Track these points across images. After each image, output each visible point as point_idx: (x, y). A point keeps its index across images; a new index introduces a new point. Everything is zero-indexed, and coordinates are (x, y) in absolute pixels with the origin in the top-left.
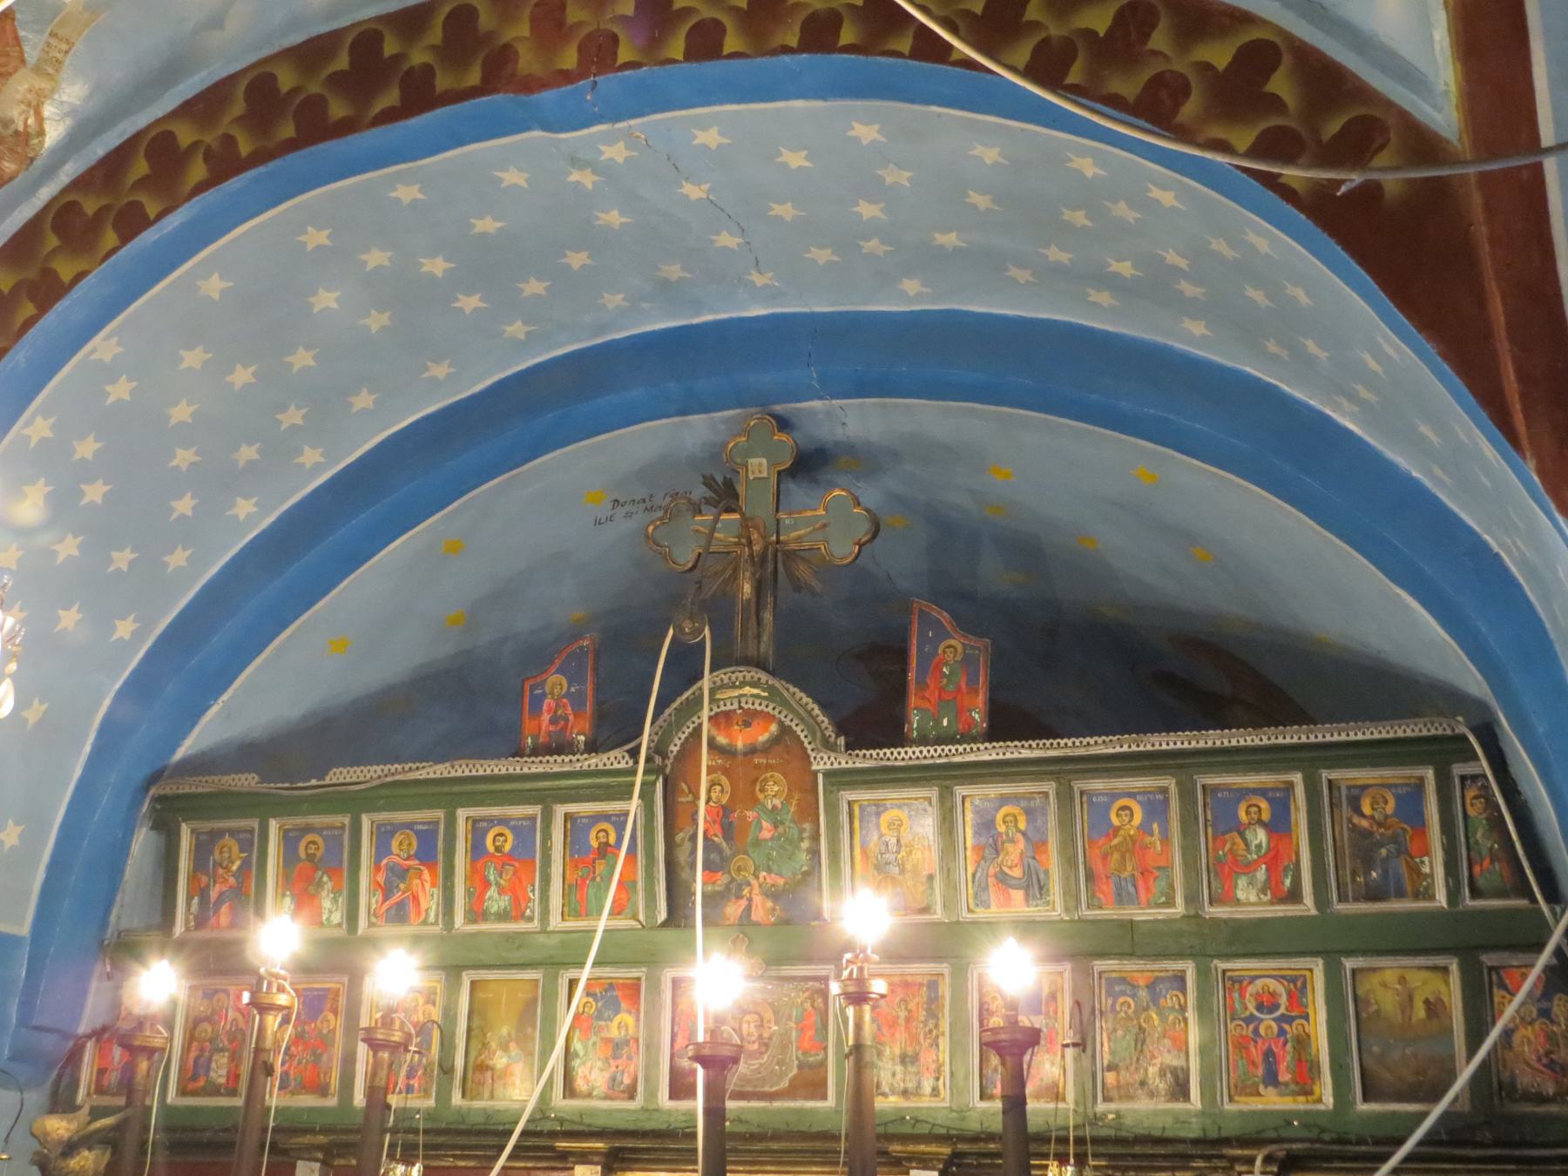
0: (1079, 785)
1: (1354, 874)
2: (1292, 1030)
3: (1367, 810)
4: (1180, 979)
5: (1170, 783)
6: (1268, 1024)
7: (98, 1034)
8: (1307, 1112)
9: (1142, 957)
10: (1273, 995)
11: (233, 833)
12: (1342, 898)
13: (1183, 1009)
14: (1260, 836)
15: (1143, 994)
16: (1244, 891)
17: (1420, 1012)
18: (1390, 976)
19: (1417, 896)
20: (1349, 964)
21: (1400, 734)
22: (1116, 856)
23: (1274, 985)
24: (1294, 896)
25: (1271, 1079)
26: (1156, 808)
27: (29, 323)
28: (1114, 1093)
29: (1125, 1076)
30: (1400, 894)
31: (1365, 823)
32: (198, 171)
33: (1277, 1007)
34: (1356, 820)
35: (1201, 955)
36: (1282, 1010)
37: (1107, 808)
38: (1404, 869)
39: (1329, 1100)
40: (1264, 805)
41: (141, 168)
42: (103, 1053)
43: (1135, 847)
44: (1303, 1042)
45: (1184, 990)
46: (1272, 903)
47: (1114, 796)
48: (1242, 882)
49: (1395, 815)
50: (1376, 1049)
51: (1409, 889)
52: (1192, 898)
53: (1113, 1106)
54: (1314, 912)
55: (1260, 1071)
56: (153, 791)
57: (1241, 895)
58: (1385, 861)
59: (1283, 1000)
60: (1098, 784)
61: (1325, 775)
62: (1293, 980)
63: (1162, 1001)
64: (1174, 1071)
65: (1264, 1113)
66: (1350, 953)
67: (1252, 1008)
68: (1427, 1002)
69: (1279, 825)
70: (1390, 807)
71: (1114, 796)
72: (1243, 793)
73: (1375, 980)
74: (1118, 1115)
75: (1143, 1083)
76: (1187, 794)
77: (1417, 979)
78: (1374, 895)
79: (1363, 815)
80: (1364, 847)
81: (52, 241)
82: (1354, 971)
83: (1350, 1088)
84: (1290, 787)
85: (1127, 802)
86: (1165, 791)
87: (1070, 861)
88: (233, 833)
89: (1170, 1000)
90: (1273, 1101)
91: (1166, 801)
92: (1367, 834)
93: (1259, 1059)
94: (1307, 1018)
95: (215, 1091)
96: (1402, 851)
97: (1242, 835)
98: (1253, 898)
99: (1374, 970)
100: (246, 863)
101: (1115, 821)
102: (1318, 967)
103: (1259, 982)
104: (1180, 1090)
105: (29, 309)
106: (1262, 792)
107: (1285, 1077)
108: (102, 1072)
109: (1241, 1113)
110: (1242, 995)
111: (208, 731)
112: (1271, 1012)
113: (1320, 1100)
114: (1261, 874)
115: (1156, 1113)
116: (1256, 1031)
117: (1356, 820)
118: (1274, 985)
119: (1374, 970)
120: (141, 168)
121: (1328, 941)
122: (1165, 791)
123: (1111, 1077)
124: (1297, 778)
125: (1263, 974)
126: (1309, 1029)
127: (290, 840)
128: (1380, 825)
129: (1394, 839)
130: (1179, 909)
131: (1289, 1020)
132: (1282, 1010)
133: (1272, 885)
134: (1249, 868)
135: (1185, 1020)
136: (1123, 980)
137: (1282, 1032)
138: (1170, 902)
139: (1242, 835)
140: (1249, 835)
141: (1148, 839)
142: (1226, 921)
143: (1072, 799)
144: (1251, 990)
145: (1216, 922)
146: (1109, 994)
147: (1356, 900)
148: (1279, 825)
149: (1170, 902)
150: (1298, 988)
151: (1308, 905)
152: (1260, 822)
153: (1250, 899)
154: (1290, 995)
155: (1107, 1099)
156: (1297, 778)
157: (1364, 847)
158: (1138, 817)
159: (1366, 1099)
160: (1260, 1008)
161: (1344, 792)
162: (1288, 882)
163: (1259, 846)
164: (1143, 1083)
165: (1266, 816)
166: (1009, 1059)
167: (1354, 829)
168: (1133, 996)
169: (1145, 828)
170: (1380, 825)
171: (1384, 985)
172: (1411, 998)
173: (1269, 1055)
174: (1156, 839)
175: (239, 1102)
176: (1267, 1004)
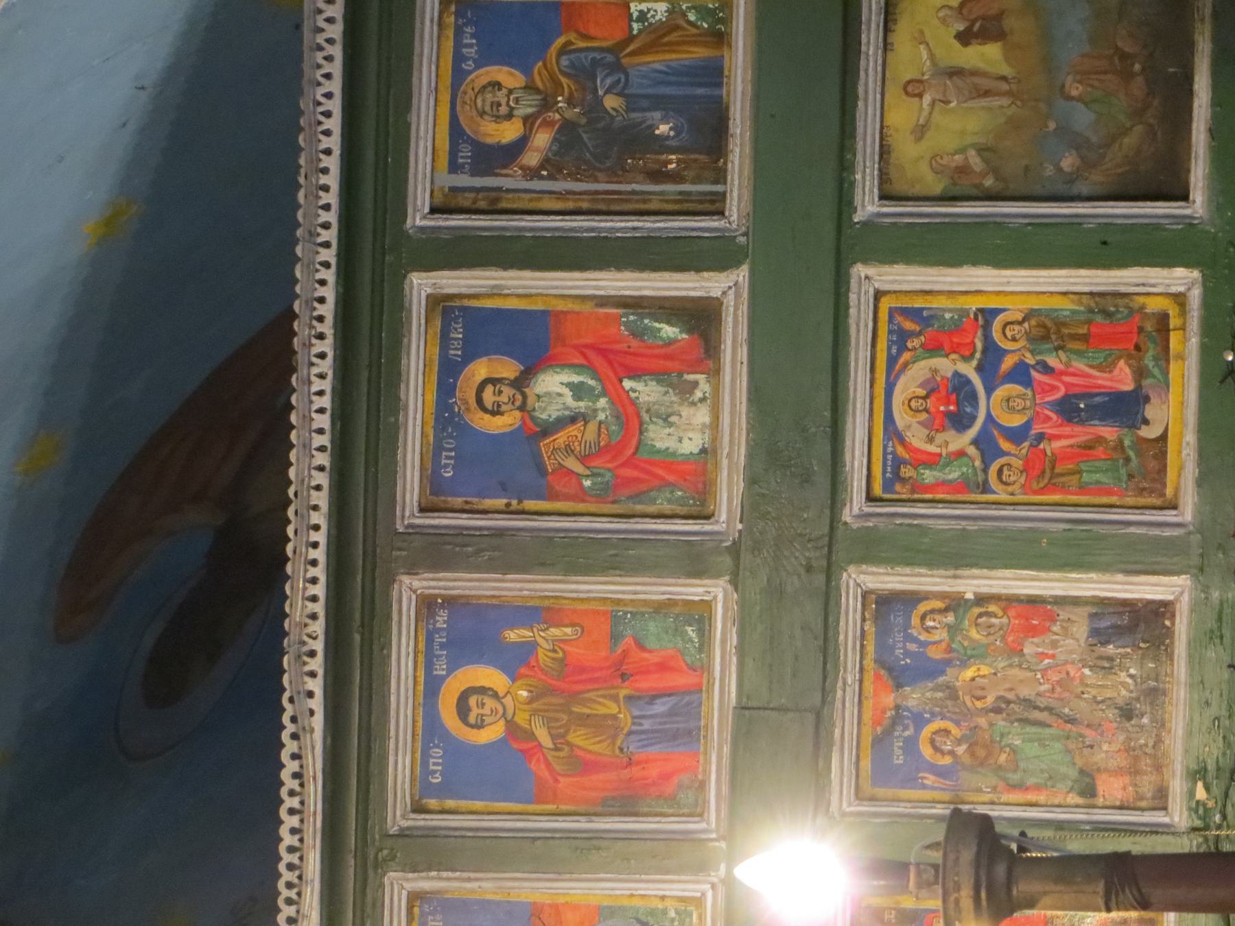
0: (398, 816)
1: (658, 175)
2: (1015, 351)
3: (509, 132)
4: (885, 605)
5: (408, 589)
6: (1002, 405)
8: (1208, 329)
9: (826, 693)
10: (932, 388)
12: (714, 206)
13: (955, 604)
14: (554, 387)
15: (914, 697)
16: (682, 432)
17: (986, 56)
18: (902, 115)
19: (720, 38)
20: (867, 206)
21: (336, 31)
22: (578, 737)
23: (909, 384)
24: (701, 317)
25: (1126, 408)
26: (468, 632)
28: (1147, 785)
29: (1108, 752)
30: (714, 74)
31: (542, 139)
33: (961, 385)
34: (532, 159)
35: (834, 549)
36: (968, 370)
37: (457, 751)
38: (657, 61)
39: (1182, 278)
40: (480, 369)
43: (564, 686)
44: (1047, 329)
45: (910, 599)
46: (715, 374)
47: (432, 729)
48: (660, 438)
49: (527, 71)
50: (1068, 162)
51: (701, 53)
52: (694, 560)
53: (1177, 786)
54: (742, 274)
55: (1109, 432)
57: (691, 445)
58: (632, 103)
59: (946, 366)
60: (400, 767)
61: (418, 218)
62: (900, 339)
63: (935, 654)
64: (1100, 636)
65: (1203, 429)
66: (844, 201)
67: (962, 441)
68: (964, 38)
69: (531, 340)
70: (509, 77)
71: (432, 729)
72: (446, 417)
73: (907, 150)
74: (1198, 773)
75: (1127, 713)
76: (440, 552)
77: (910, 58)
78: (710, 133)
79: (519, 146)
80: (599, 148)
82: (885, 197)
83: (1154, 227)
84: (441, 305)
85: (443, 702)
86: (428, 605)
87: (584, 851)
89: (934, 634)
90: (1177, 410)
91: (450, 602)
92: (567, 134)
93: (1081, 434)
94: (989, 314)
96: (613, 60)
97: (547, 430)
98: (702, 416)
99: (885, 151)
101: (492, 733)
102: (870, 277)
103: (901, 418)
104: (1143, 624)
106: (449, 372)
107: (1123, 378)
109: (1200, 482)
110: (932, 461)
112: (973, 397)
113: (1180, 299)
114: (645, 391)
115: (1198, 683)
116: (1016, 435)
117: (532, 159)
118: (909, 384)
119: (885, 151)
121: (815, 244)
122: (428, 605)
123: (1112, 788)
124: (422, 285)
125: (884, 405)
126: (1015, 309)
128: (547, 104)
129: (584, 74)
130: (716, 592)
131: (991, 358)
132: (968, 370)
133: (666, 367)
134: (631, 417)
135: (981, 600)
136: (881, 742)
137: (1020, 374)
138: (699, 614)
139: (547, 430)
140: (549, 413)
141: (543, 656)
142: (752, 481)
143: (431, 834)
144: (917, 437)
145: (754, 507)
146: (911, 781)
147: (720, 176)
148: (531, 340)
149: (699, 614)
150: (915, 327)
151: (724, 286)
152: (520, 383)
153: (703, 423)
154: (933, 348)
155: (1161, 801)
156: (422, 285)
157: (599, 148)
158: (489, 676)
159: (1183, 196)
160: (960, 422)
161: (464, 180)
162: (669, 331)
163: (578, 391)
164: (1127, 713)
165: (508, 369)
166: (1022, 888)
167: (552, 166)
168: (920, 721)
169: (516, 661)
170: (547, 104)
171: (920, 131)
172: (956, 73)
173: (1068, 410)
174: (546, 638)
176: (954, 401)
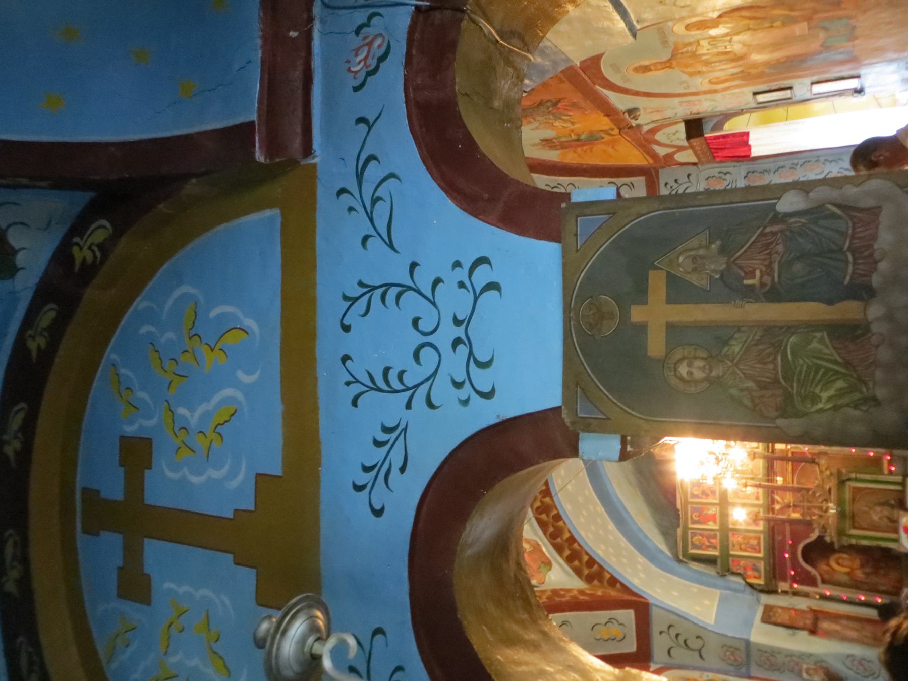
7: (744, 579)
11: (692, 538)
27: (579, 545)
32: (547, 500)
41: (544, 516)
42: (750, 577)
56: (681, 558)
81: (559, 540)
88: (692, 538)
95: (759, 543)
100: (700, 535)
105: (575, 545)
108: (755, 577)
111: (664, 548)
120: (544, 516)
127: (694, 522)
175: (762, 536)
